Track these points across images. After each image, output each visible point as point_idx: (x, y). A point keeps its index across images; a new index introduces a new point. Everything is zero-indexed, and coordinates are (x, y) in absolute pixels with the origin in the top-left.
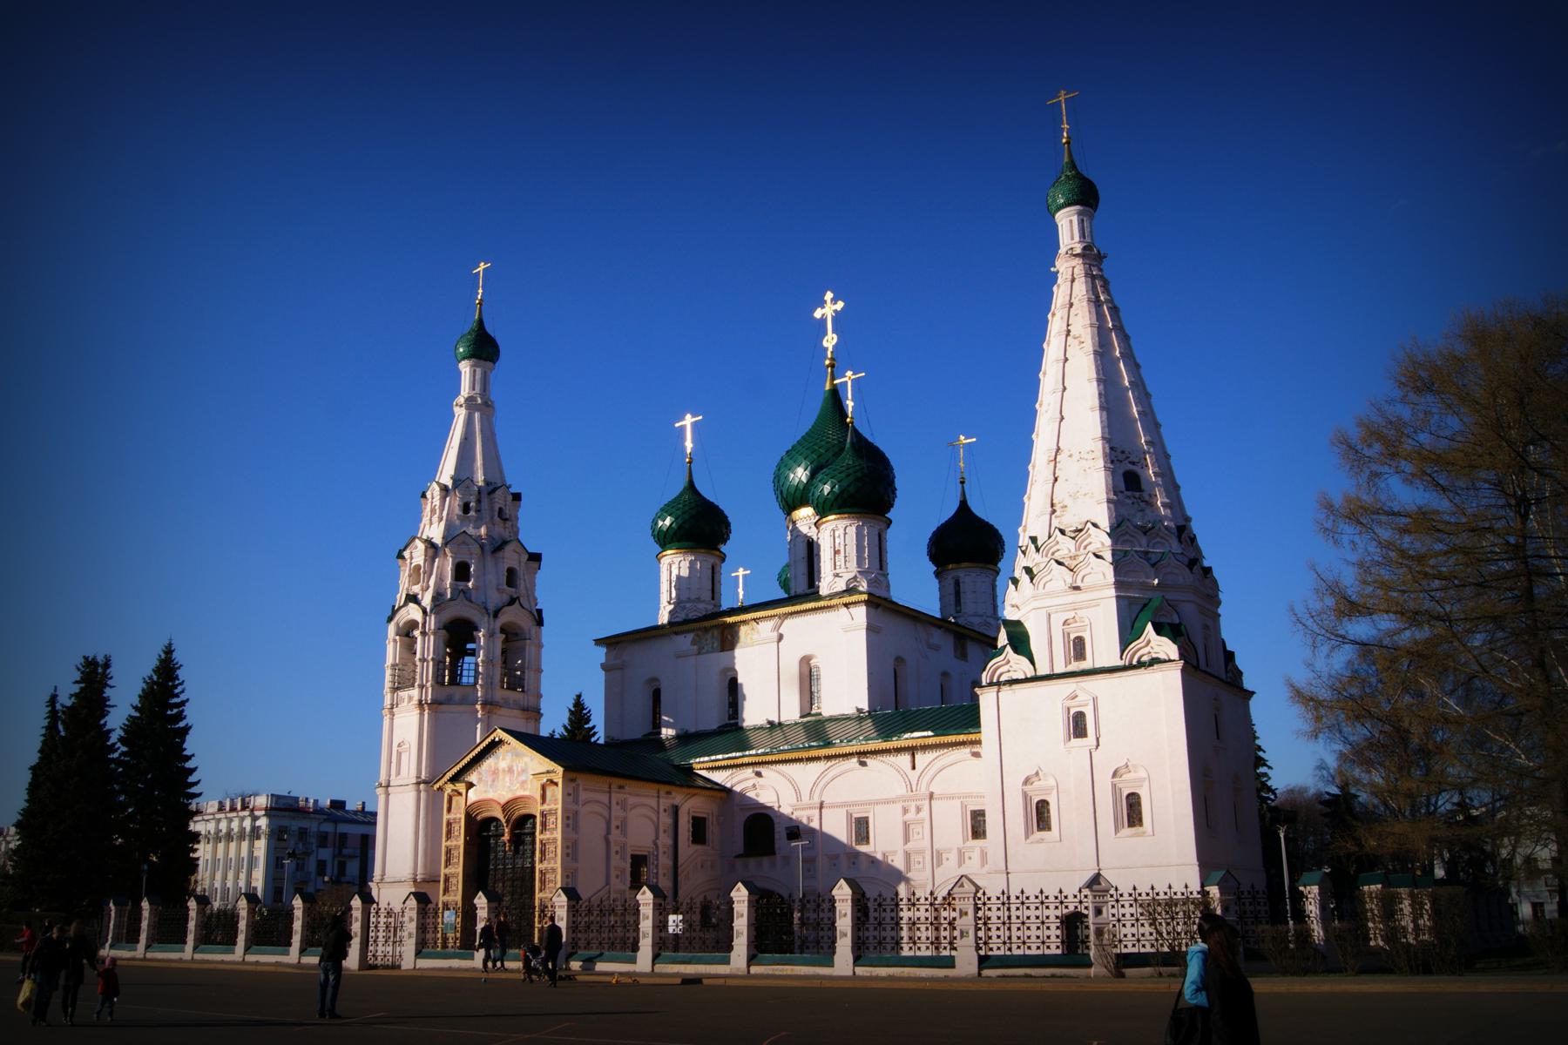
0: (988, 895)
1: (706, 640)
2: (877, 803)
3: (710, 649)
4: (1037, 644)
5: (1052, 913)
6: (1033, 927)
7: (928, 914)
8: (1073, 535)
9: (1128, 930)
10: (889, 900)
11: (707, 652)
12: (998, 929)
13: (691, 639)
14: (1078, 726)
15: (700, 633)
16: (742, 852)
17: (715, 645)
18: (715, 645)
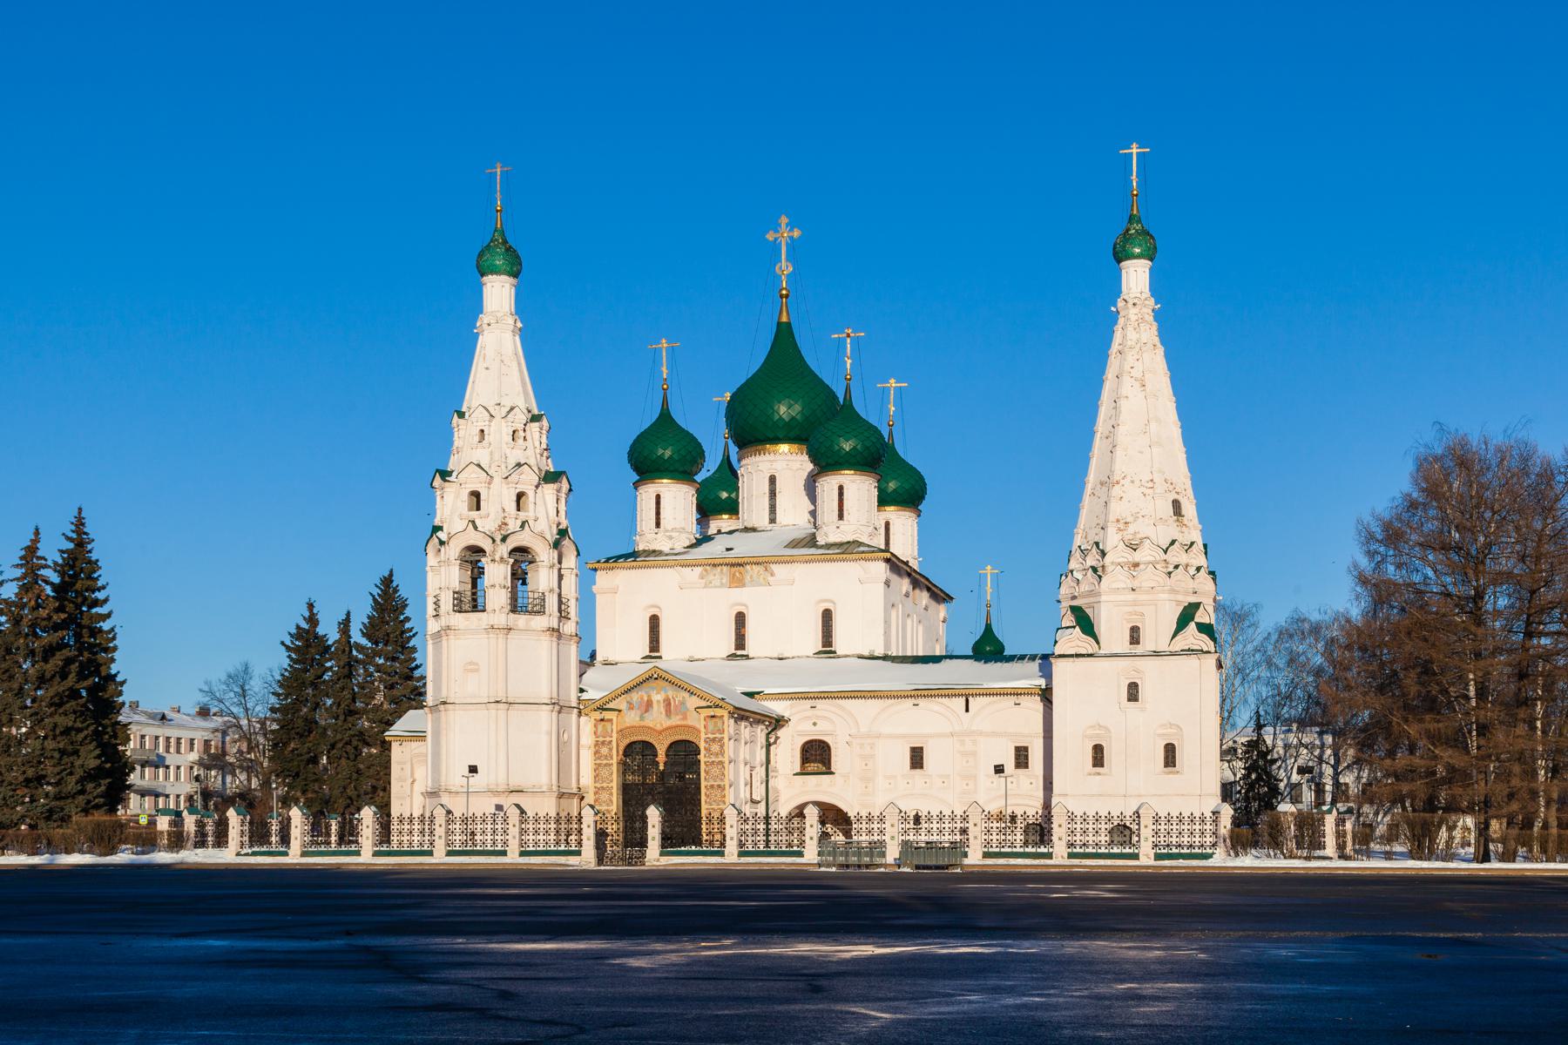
0: (992, 813)
1: (715, 575)
2: (932, 736)
3: (718, 584)
4: (1102, 628)
5: (1103, 826)
6: (1174, 836)
7: (1211, 827)
8: (1135, 547)
9: (1162, 839)
10: (1175, 817)
11: (716, 587)
12: (1165, 836)
13: (699, 573)
14: (1133, 693)
15: (708, 567)
16: (799, 771)
17: (724, 581)
18: (724, 581)
